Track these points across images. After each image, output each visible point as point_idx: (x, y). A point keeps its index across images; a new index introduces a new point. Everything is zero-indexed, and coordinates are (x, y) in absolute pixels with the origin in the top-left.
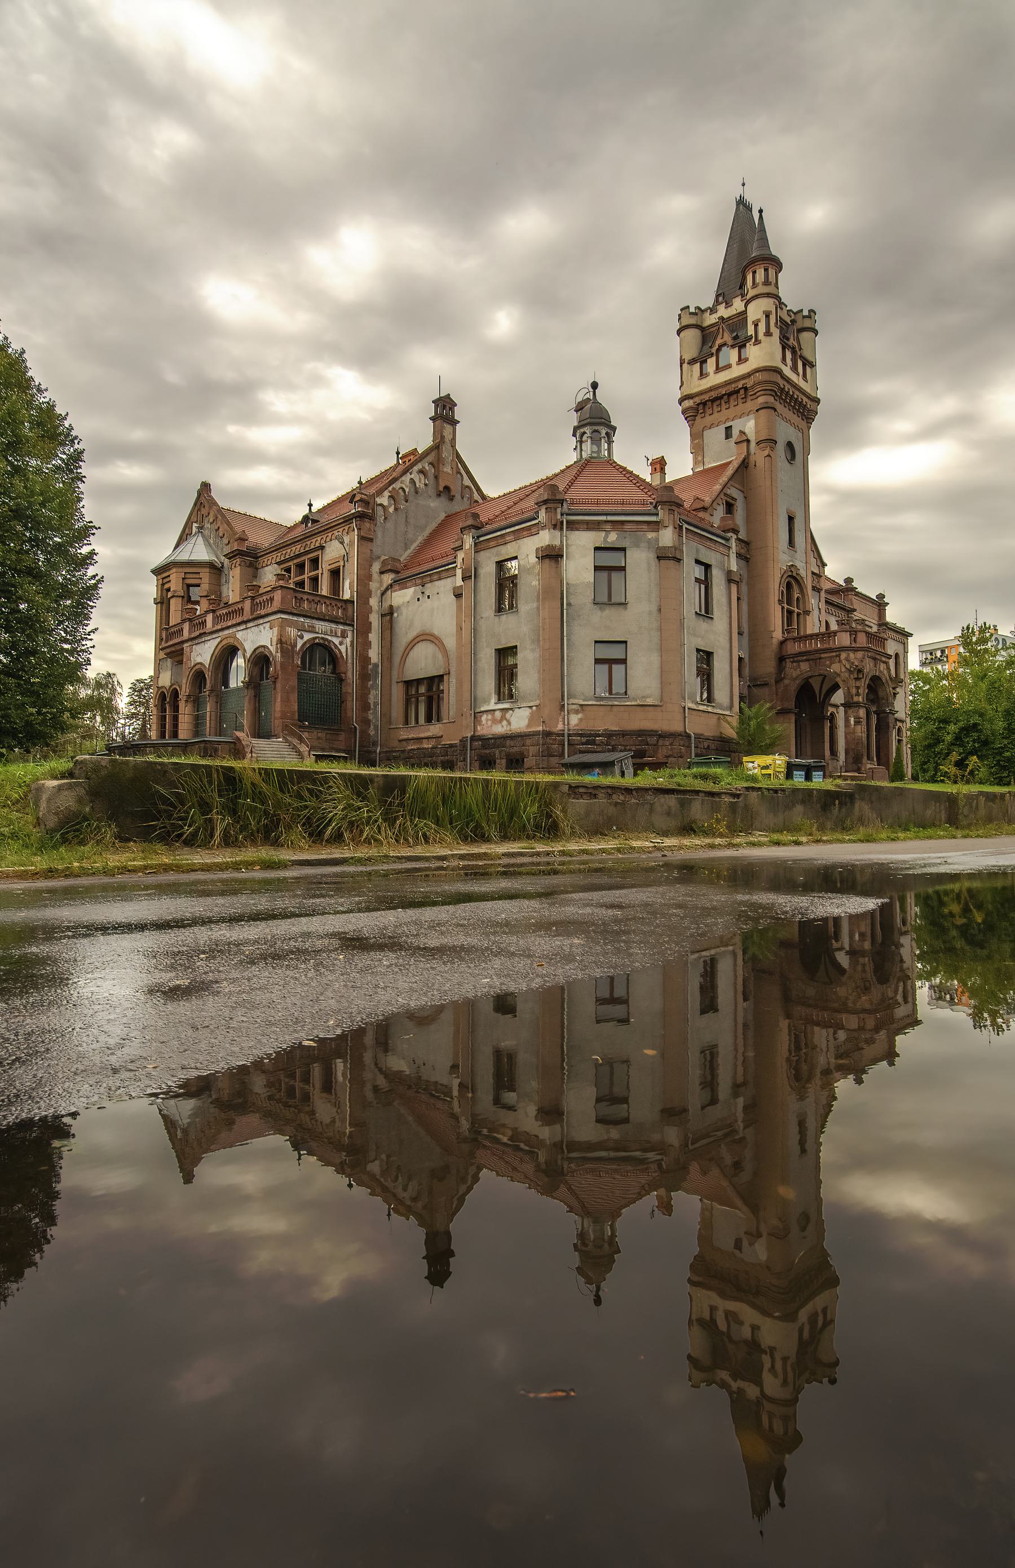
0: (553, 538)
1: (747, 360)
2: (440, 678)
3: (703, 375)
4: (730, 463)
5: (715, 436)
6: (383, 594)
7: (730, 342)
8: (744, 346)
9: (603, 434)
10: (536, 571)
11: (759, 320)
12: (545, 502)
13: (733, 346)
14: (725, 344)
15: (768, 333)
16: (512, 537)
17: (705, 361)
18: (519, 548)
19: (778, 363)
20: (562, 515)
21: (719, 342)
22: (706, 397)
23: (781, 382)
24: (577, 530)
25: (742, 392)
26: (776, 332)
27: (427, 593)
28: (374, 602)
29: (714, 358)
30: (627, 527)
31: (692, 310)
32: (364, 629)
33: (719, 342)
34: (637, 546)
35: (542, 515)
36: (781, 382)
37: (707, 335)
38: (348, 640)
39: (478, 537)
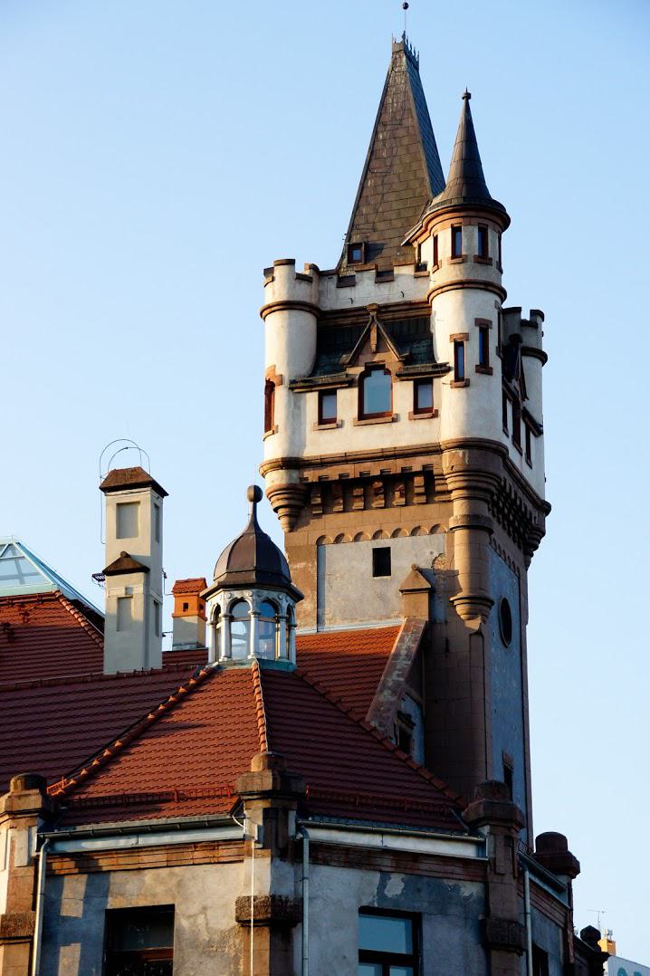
0: (276, 880)
3: (325, 421)
4: (391, 633)
5: (348, 564)
8: (429, 382)
9: (284, 613)
10: (230, 952)
11: (466, 336)
13: (402, 376)
15: (484, 368)
16: (161, 857)
17: (333, 392)
18: (180, 884)
20: (299, 828)
22: (333, 473)
23: (504, 474)
24: (326, 863)
25: (419, 481)
26: (496, 362)
29: (353, 393)
30: (424, 866)
31: (300, 268)
34: (443, 912)
36: (504, 474)
39: (54, 840)
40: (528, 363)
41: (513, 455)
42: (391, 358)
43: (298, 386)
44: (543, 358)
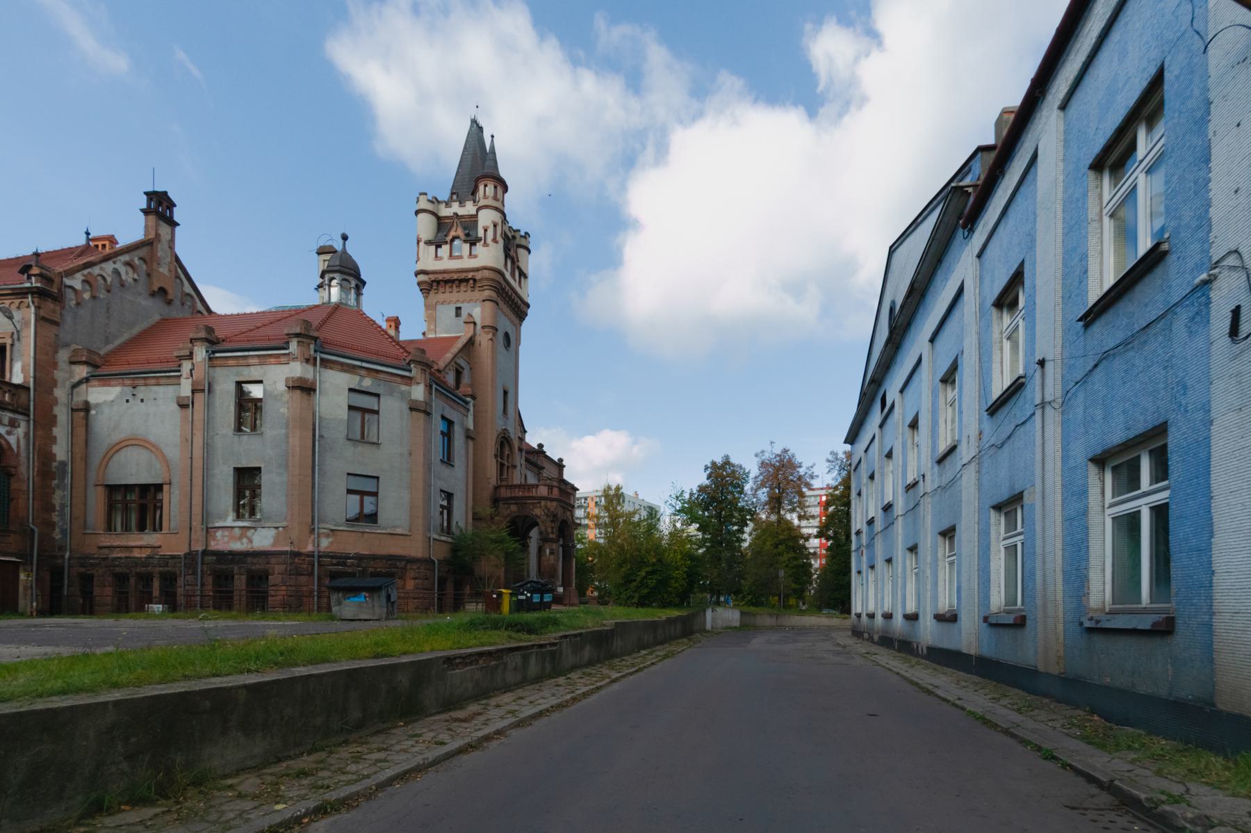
1: (476, 257)
2: (158, 488)
6: (74, 386)
7: (463, 237)
12: (297, 335)
13: (465, 241)
14: (458, 237)
19: (500, 266)
21: (452, 233)
27: (140, 396)
28: (60, 393)
32: (46, 421)
33: (452, 233)
35: (294, 346)
37: (442, 224)
38: (20, 431)
40: (521, 252)
41: (508, 276)
42: (460, 232)
43: (429, 243)
44: (529, 252)
